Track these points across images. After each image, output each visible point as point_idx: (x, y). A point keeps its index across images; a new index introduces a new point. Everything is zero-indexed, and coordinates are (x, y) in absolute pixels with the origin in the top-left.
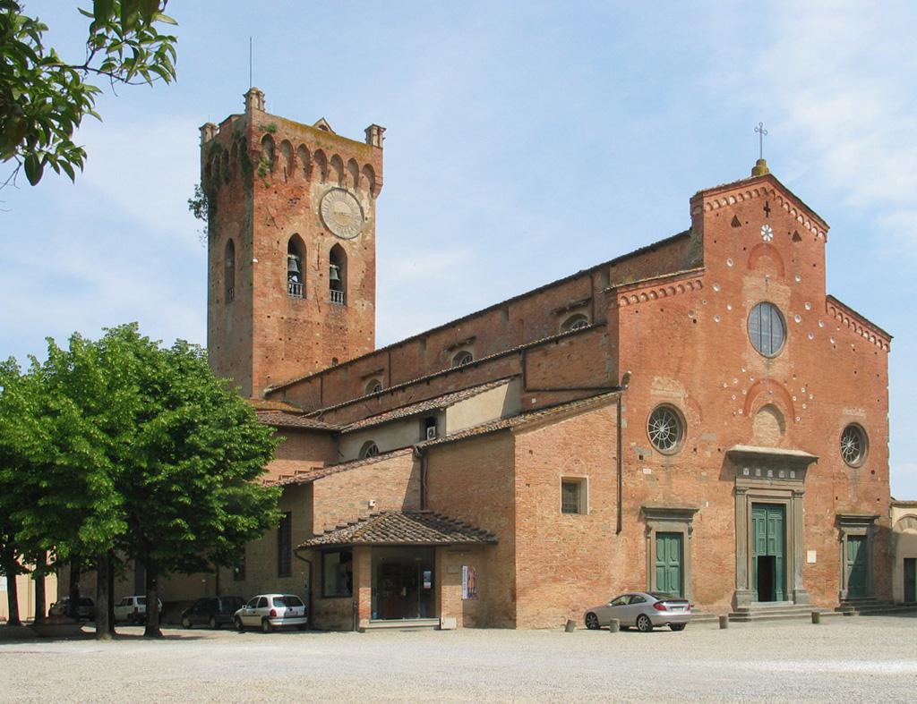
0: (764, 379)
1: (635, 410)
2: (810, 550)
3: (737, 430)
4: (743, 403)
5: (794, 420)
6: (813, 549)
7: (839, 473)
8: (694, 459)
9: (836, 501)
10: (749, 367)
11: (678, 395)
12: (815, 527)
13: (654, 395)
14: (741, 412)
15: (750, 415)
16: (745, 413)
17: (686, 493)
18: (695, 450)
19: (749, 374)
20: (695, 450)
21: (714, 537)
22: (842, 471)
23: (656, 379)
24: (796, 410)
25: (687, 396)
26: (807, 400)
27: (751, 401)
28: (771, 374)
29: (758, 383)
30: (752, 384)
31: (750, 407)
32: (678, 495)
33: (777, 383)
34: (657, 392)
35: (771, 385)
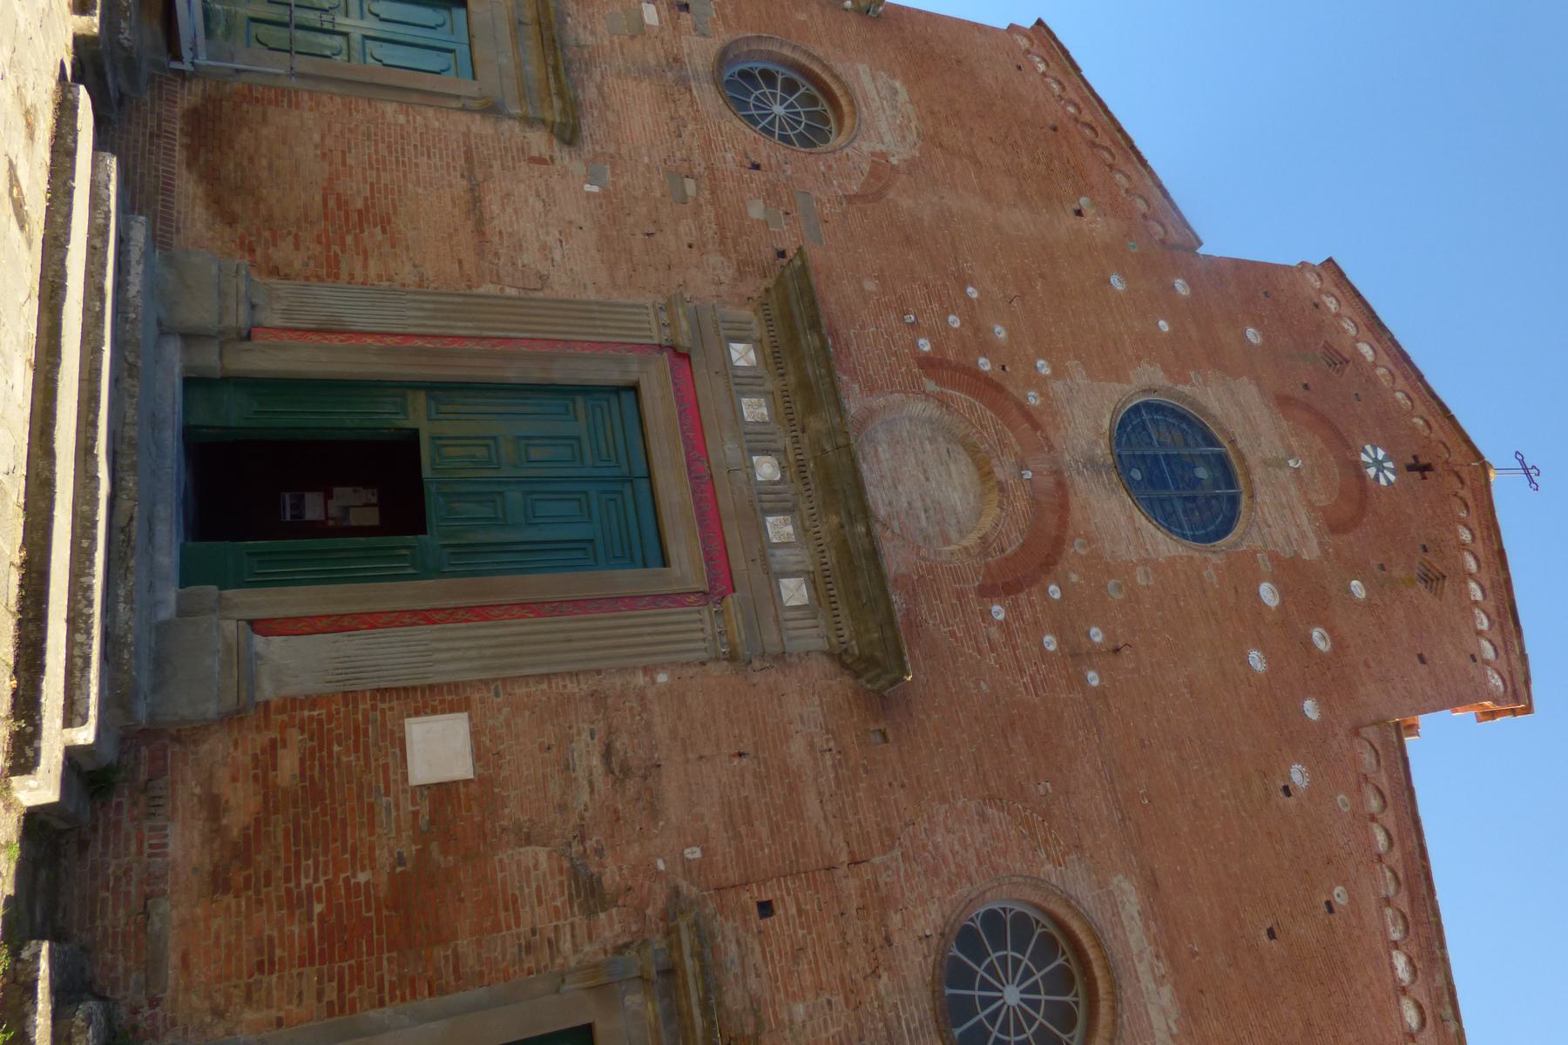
0: (1051, 448)
1: (802, 17)
2: (475, 734)
3: (863, 327)
4: (951, 355)
5: (988, 591)
6: (478, 755)
7: (885, 903)
8: (729, 160)
9: (749, 898)
10: (1058, 386)
11: (888, 138)
12: (596, 761)
13: (857, 74)
14: (925, 345)
15: (931, 386)
16: (929, 364)
17: (611, 117)
18: (756, 167)
19: (1040, 383)
20: (756, 167)
21: (475, 202)
22: (896, 920)
23: (897, 84)
24: (1022, 596)
25: (894, 161)
26: (1077, 654)
27: (970, 393)
28: (1078, 480)
29: (1027, 414)
30: (1011, 389)
31: (955, 385)
32: (599, 88)
33: (1064, 507)
34: (866, 78)
35: (1048, 482)
